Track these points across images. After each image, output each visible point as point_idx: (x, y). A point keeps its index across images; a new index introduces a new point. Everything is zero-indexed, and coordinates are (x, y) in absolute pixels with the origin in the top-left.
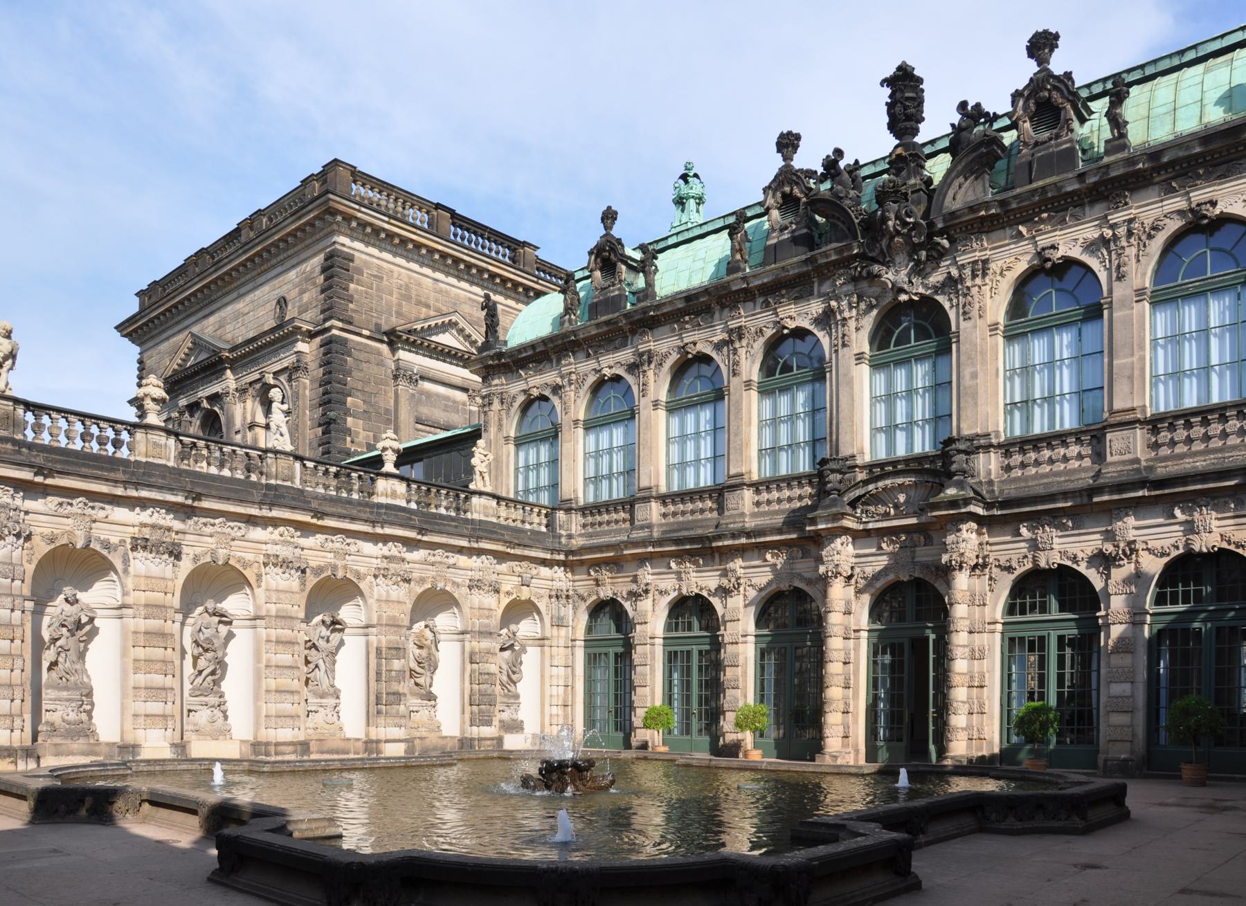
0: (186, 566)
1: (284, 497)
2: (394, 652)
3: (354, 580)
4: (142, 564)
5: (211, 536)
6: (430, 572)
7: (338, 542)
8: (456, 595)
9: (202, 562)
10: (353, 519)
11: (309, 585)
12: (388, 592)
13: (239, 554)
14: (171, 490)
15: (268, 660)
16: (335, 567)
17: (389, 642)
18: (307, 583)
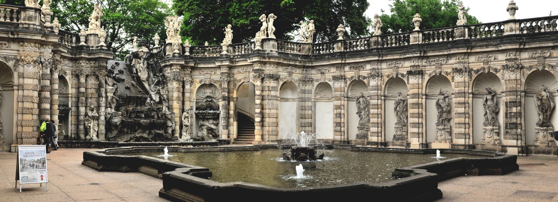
0: (427, 78)
1: (458, 44)
2: (513, 104)
3: (494, 72)
4: (413, 80)
5: (434, 65)
6: (535, 62)
7: (484, 57)
8: (552, 72)
9: (432, 75)
10: (487, 46)
11: (473, 78)
12: (509, 75)
13: (445, 70)
14: (415, 52)
15: (456, 111)
16: (484, 69)
17: (510, 99)
18: (473, 77)
